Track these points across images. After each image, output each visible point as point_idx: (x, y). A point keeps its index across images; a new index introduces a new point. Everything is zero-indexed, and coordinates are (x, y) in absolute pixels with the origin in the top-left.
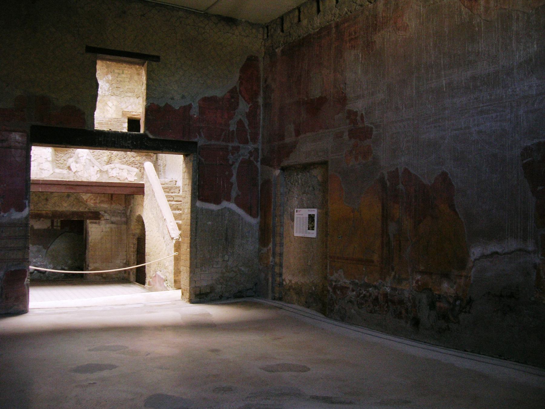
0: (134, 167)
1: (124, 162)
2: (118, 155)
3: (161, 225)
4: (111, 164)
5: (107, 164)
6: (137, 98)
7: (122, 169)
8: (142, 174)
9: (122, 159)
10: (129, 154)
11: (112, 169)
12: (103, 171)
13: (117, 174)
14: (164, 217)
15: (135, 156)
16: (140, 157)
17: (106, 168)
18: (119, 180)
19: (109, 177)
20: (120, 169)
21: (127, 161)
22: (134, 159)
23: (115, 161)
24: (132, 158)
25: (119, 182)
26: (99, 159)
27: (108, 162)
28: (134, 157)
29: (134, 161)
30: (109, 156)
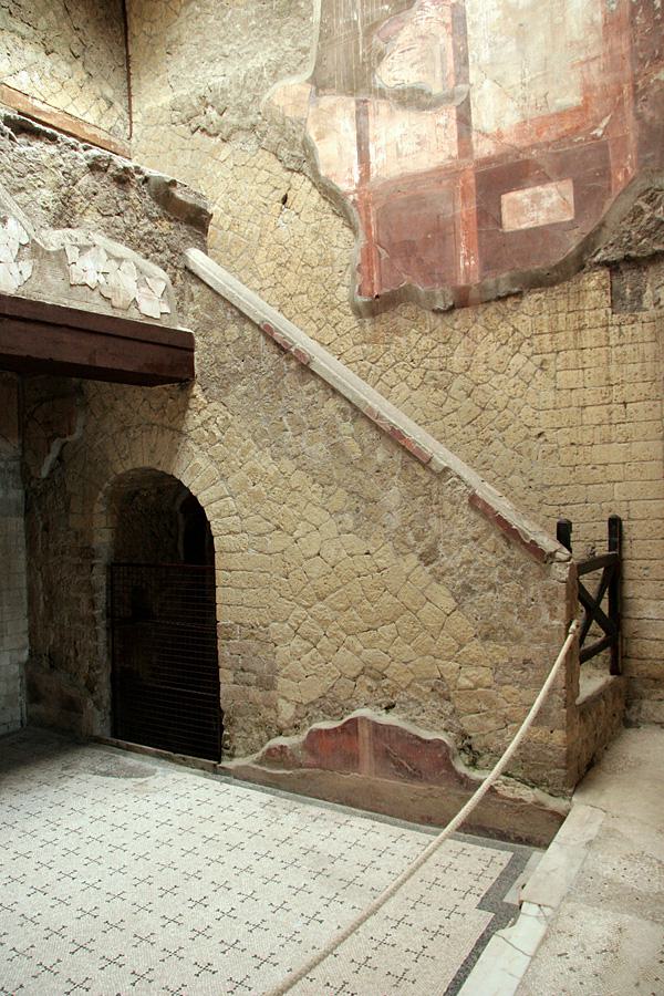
0: (154, 261)
1: (117, 230)
2: (95, 194)
3: (393, 496)
4: (70, 227)
5: (55, 226)
6: (48, 53)
7: (120, 260)
8: (177, 294)
9: (111, 215)
10: (136, 202)
11: (83, 249)
12: (43, 250)
13: (102, 279)
14: (435, 456)
15: (155, 214)
16: (173, 225)
17: (54, 238)
18: (106, 304)
19: (72, 285)
20: (110, 256)
21: (128, 229)
22: (150, 227)
23: (88, 219)
24: (146, 220)
25: (108, 312)
26: (21, 189)
27: (60, 217)
28: (152, 219)
29: (154, 236)
30: (64, 190)
